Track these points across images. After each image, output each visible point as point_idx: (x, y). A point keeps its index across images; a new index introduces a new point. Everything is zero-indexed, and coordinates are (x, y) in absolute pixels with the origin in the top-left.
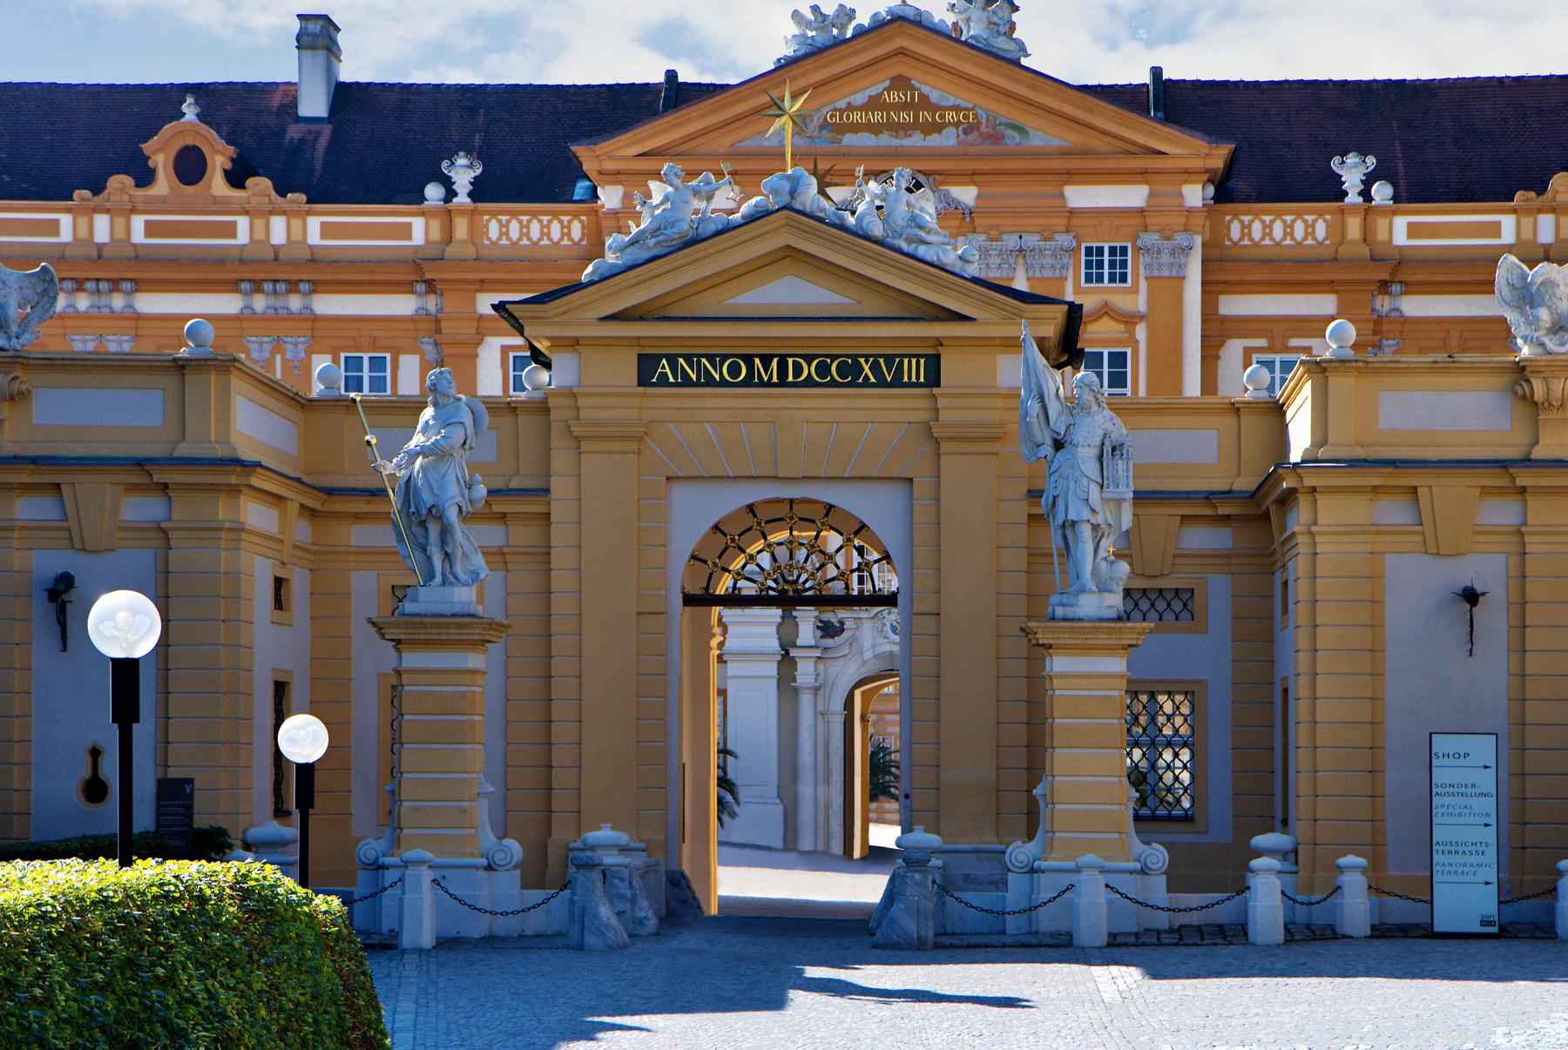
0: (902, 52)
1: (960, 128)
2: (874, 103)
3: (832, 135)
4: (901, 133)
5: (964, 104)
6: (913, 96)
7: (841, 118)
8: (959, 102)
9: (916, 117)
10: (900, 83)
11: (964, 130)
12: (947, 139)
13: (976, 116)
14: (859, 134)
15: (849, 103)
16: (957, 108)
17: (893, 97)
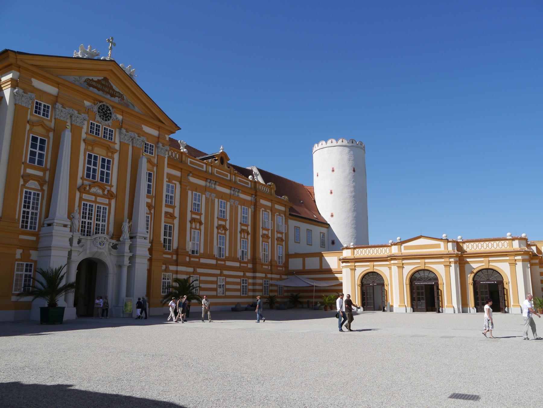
0: (111, 70)
1: (120, 99)
2: (98, 81)
3: (87, 85)
4: (105, 93)
5: (121, 93)
6: (109, 84)
7: (90, 82)
8: (119, 91)
9: (109, 91)
10: (106, 79)
11: (120, 99)
12: (116, 99)
13: (123, 97)
14: (94, 89)
15: (92, 79)
16: (119, 92)
17: (104, 82)
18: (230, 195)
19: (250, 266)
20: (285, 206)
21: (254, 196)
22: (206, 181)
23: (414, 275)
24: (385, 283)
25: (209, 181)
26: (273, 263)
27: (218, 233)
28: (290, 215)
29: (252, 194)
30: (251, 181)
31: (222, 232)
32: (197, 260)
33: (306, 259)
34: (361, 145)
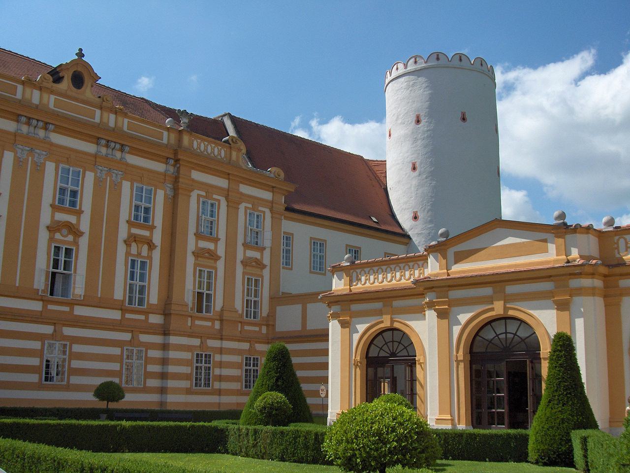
18: (95, 156)
19: (156, 319)
20: (272, 189)
21: (172, 162)
22: (18, 121)
23: (480, 334)
24: (417, 358)
25: (24, 119)
26: (227, 316)
27: (51, 239)
28: (288, 209)
29: (167, 158)
30: (168, 129)
31: (66, 239)
32: (142, 317)
33: (309, 306)
34: (482, 65)
